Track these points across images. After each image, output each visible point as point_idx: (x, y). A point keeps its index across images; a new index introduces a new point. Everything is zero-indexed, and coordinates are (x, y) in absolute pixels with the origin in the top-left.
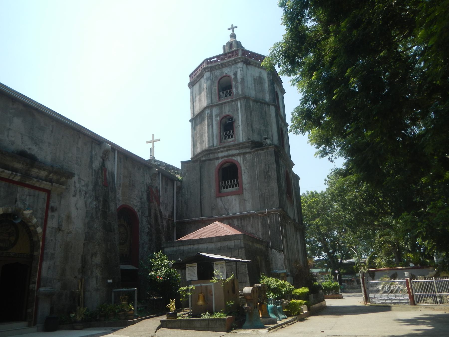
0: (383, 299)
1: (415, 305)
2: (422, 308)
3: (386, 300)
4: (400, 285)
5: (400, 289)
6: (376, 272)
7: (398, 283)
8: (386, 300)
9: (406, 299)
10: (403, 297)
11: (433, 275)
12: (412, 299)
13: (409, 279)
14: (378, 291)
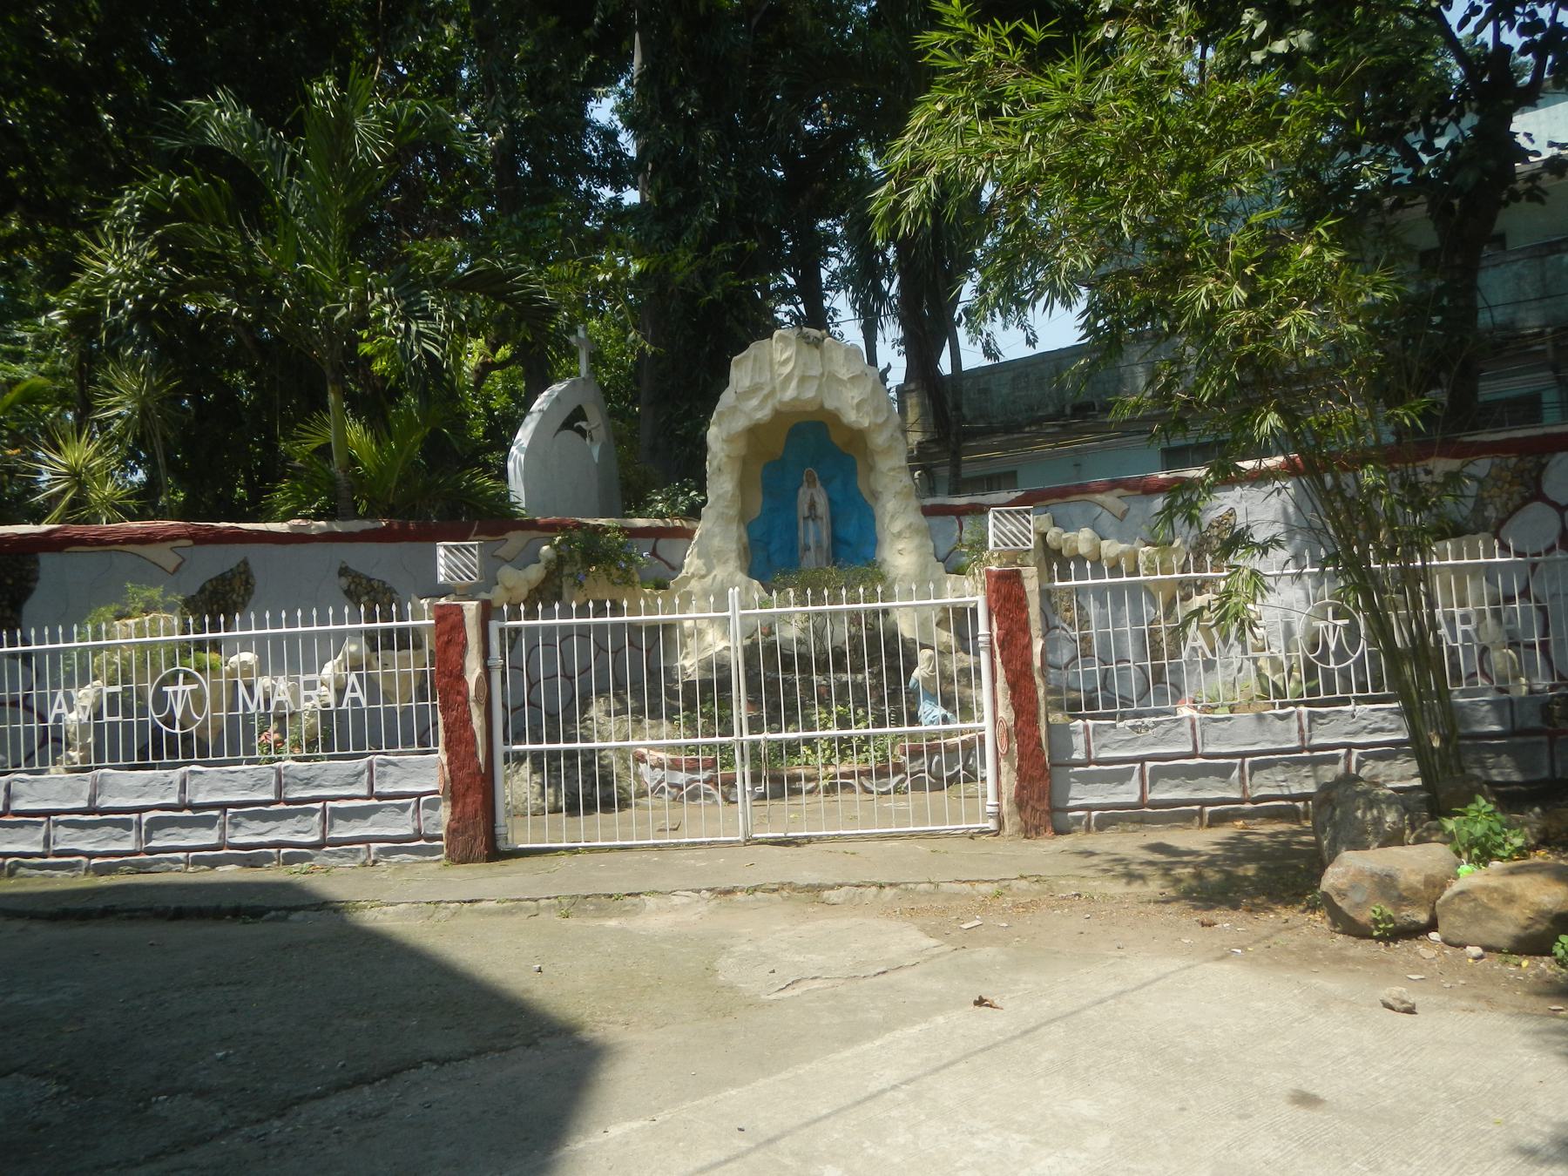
0: (121, 818)
1: (496, 853)
2: (676, 900)
3: (156, 824)
4: (278, 669)
5: (342, 715)
6: (47, 560)
7: (249, 657)
8: (156, 824)
9: (404, 808)
10: (364, 792)
11: (523, 592)
12: (474, 800)
13: (471, 608)
14: (52, 742)
